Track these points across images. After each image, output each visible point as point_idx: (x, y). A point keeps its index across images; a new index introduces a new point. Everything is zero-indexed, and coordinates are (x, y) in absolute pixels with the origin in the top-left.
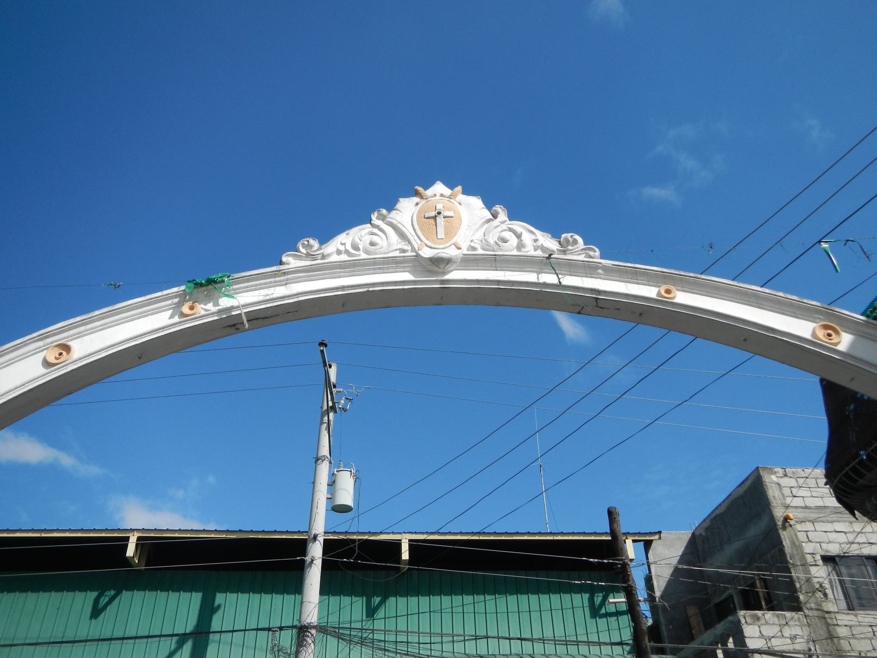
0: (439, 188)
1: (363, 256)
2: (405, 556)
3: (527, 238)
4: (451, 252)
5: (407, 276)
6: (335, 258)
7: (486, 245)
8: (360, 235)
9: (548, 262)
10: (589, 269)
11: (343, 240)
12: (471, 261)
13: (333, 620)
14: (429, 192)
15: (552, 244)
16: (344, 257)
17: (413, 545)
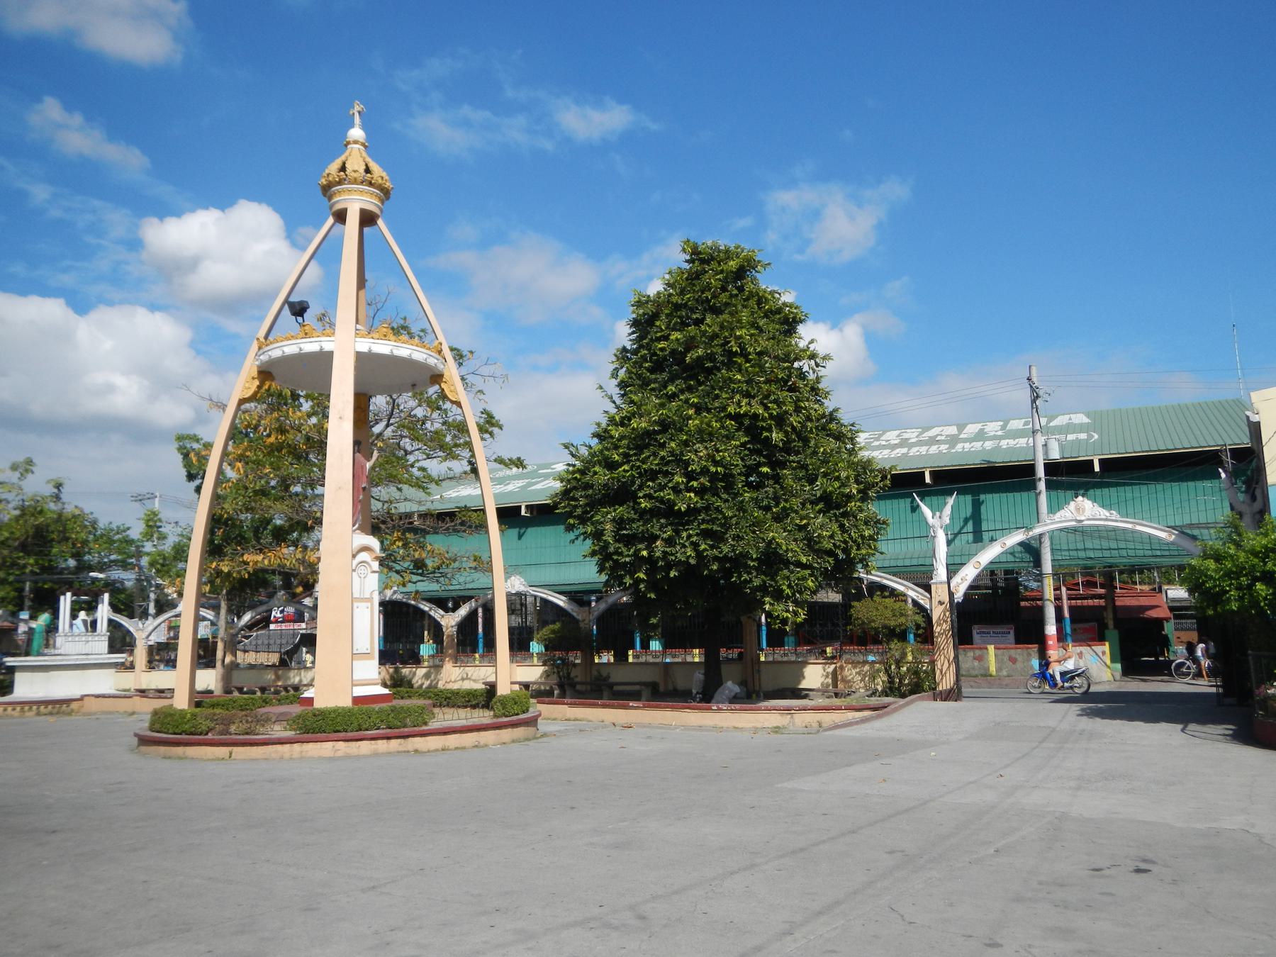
1: (1063, 519)
2: (1097, 469)
3: (1102, 513)
4: (1083, 518)
5: (1075, 523)
6: (1057, 520)
7: (1092, 515)
9: (1106, 520)
11: (1058, 515)
14: (1077, 500)
15: (1108, 514)
16: (1059, 520)
17: (1101, 461)
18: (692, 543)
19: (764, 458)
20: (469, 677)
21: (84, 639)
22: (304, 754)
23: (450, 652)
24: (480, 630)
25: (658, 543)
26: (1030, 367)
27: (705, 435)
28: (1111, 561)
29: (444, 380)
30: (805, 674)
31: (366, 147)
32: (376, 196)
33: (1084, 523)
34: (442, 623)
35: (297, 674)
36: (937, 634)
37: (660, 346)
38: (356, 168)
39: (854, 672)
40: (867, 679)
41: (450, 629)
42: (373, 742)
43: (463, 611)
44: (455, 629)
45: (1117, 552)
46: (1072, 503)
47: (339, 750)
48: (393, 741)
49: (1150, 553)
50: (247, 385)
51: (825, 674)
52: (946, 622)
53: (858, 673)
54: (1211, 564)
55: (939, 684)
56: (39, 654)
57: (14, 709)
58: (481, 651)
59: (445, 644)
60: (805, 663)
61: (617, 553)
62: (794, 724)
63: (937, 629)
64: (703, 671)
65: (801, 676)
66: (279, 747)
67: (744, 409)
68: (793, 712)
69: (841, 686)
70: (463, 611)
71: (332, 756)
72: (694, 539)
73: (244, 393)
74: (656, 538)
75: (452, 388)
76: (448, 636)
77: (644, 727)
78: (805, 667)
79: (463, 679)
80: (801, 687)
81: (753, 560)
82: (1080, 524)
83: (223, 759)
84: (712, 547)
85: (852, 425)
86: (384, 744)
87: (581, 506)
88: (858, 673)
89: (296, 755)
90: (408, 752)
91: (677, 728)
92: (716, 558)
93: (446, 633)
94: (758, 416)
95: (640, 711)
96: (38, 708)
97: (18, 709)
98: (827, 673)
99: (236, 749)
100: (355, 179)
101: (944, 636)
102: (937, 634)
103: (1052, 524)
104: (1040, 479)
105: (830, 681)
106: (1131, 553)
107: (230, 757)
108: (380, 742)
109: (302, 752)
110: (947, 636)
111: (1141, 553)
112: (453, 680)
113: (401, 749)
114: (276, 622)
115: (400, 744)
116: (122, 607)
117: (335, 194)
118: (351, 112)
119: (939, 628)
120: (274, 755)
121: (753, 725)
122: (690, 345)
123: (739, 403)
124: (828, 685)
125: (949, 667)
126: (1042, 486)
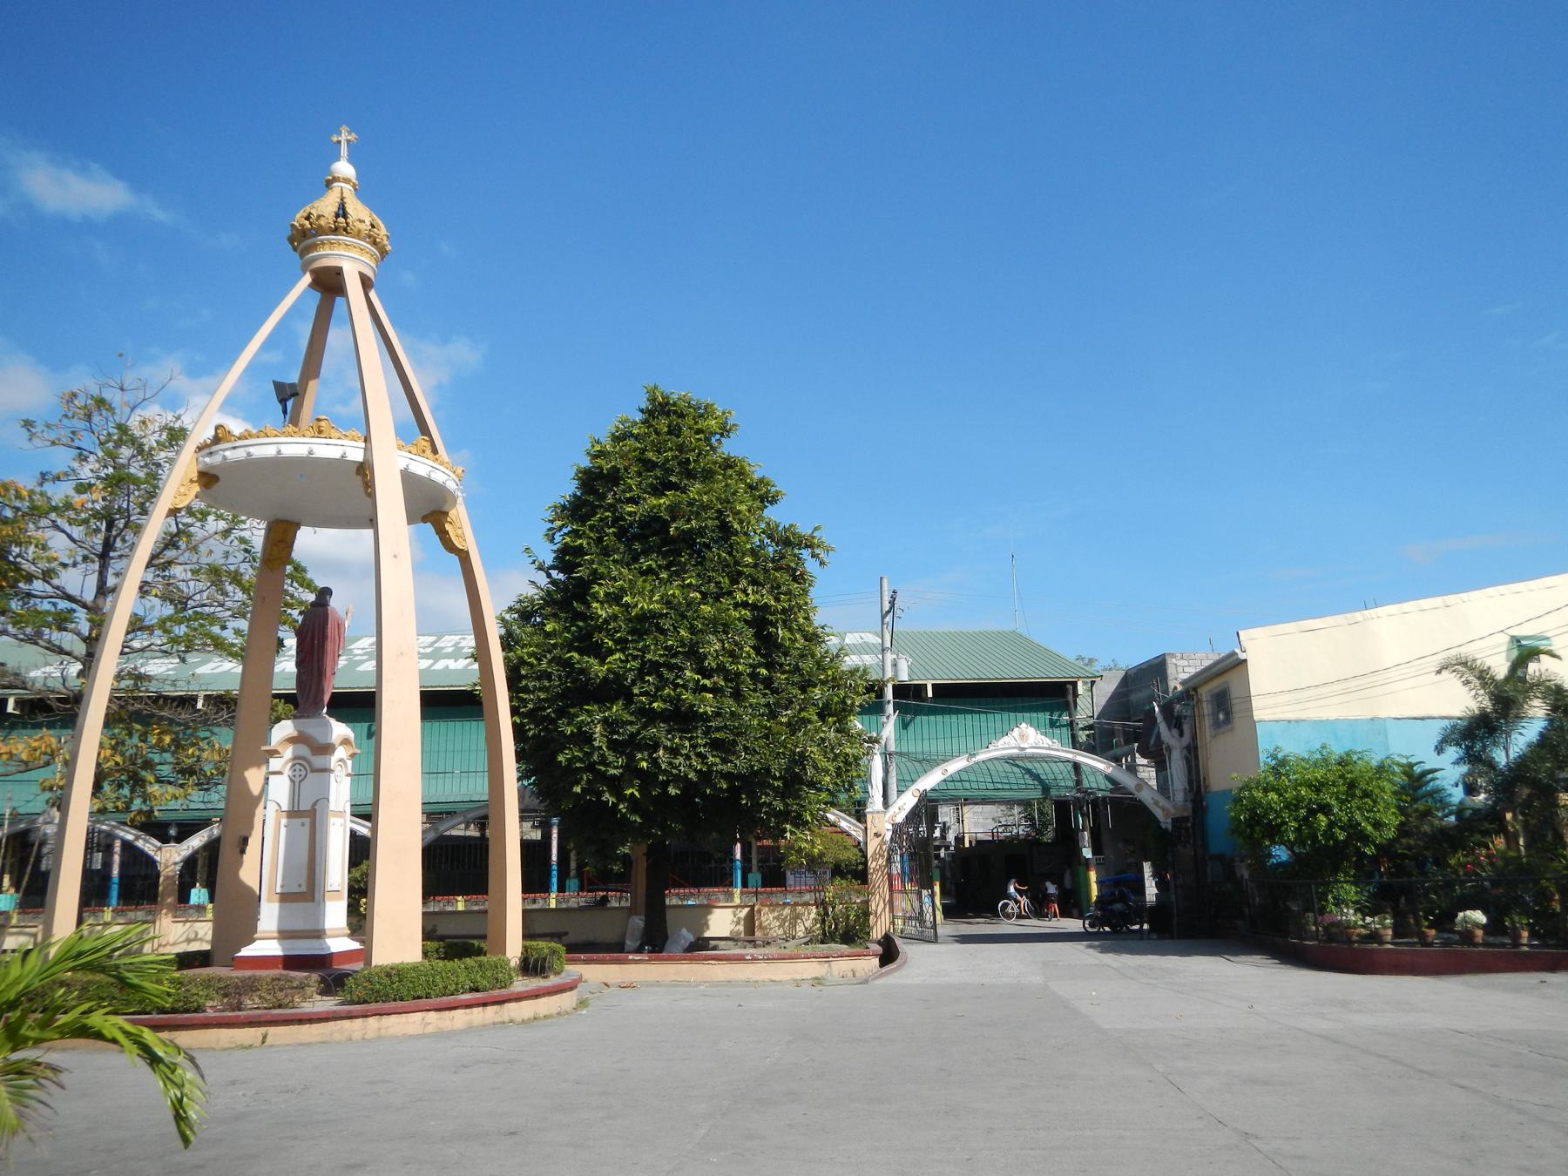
0: (1024, 725)
1: (1007, 746)
2: (930, 694)
5: (1016, 751)
8: (1006, 739)
9: (1049, 749)
10: (1058, 750)
11: (1002, 741)
12: (1031, 747)
13: (904, 750)
15: (1050, 743)
18: (699, 755)
19: (761, 657)
20: (199, 936)
22: (383, 1031)
23: (169, 900)
24: (554, 858)
25: (661, 753)
26: (881, 578)
27: (720, 626)
28: (953, 793)
29: (449, 519)
30: (710, 923)
31: (355, 190)
32: (375, 259)
33: (1028, 751)
34: (158, 858)
36: (872, 871)
37: (629, 509)
38: (362, 218)
39: (771, 916)
40: (787, 924)
41: (172, 867)
42: (468, 1011)
43: (196, 841)
44: (178, 867)
45: (960, 784)
46: (1016, 729)
47: (429, 1024)
48: (489, 1008)
49: (990, 786)
50: (182, 490)
51: (735, 920)
52: (882, 856)
53: (776, 918)
54: (1273, 796)
55: (872, 928)
58: (114, 900)
59: (161, 888)
60: (708, 908)
61: (604, 761)
62: (831, 975)
63: (872, 865)
64: (643, 918)
65: (706, 925)
66: (346, 1024)
67: (753, 598)
68: (831, 959)
69: (758, 934)
70: (196, 841)
71: (421, 1032)
72: (702, 749)
73: (177, 501)
74: (655, 746)
75: (459, 532)
76: (167, 878)
77: (652, 985)
78: (710, 913)
79: (189, 941)
80: (707, 934)
81: (775, 778)
82: (1022, 752)
83: (251, 1046)
84: (725, 761)
85: (823, 628)
86: (479, 1013)
87: (532, 700)
88: (776, 918)
89: (370, 1034)
90: (504, 1023)
91: (700, 985)
92: (727, 776)
93: (162, 874)
94: (770, 607)
95: (642, 967)
98: (739, 918)
99: (272, 1030)
100: (359, 231)
101: (880, 873)
102: (872, 871)
103: (995, 750)
104: (889, 702)
105: (741, 928)
106: (975, 786)
107: (263, 1042)
108: (475, 1010)
109: (379, 1029)
110: (883, 872)
111: (982, 786)
112: (171, 942)
113: (498, 1019)
115: (496, 1013)
117: (323, 244)
118: (335, 139)
119: (874, 864)
120: (337, 1036)
121: (792, 976)
122: (675, 512)
123: (744, 591)
124: (738, 933)
125: (884, 908)
126: (890, 708)
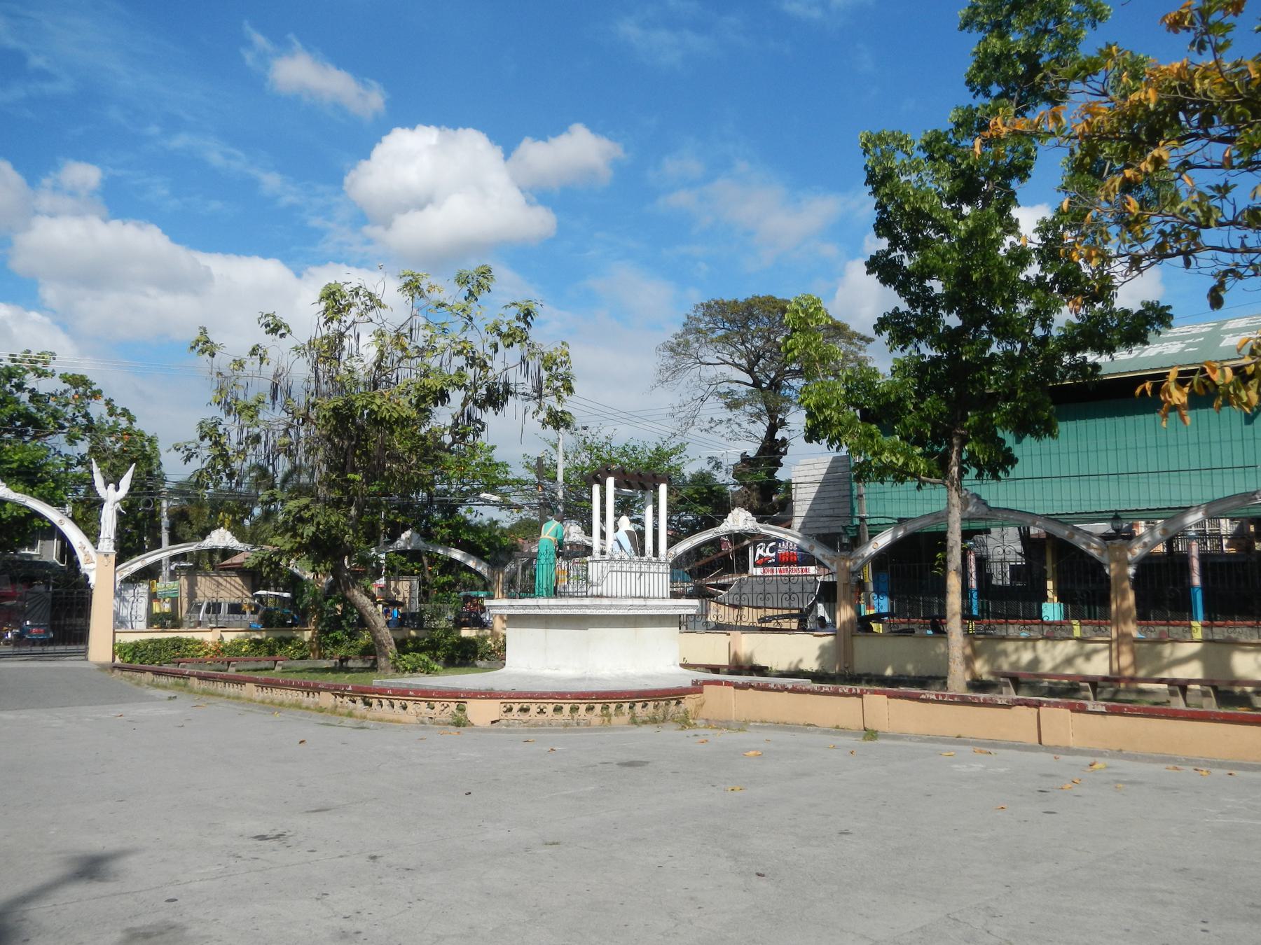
21: (635, 567)
35: (1025, 648)
56: (555, 593)
57: (590, 709)
96: (630, 708)
97: (598, 707)
114: (763, 563)
116: (487, 549)
